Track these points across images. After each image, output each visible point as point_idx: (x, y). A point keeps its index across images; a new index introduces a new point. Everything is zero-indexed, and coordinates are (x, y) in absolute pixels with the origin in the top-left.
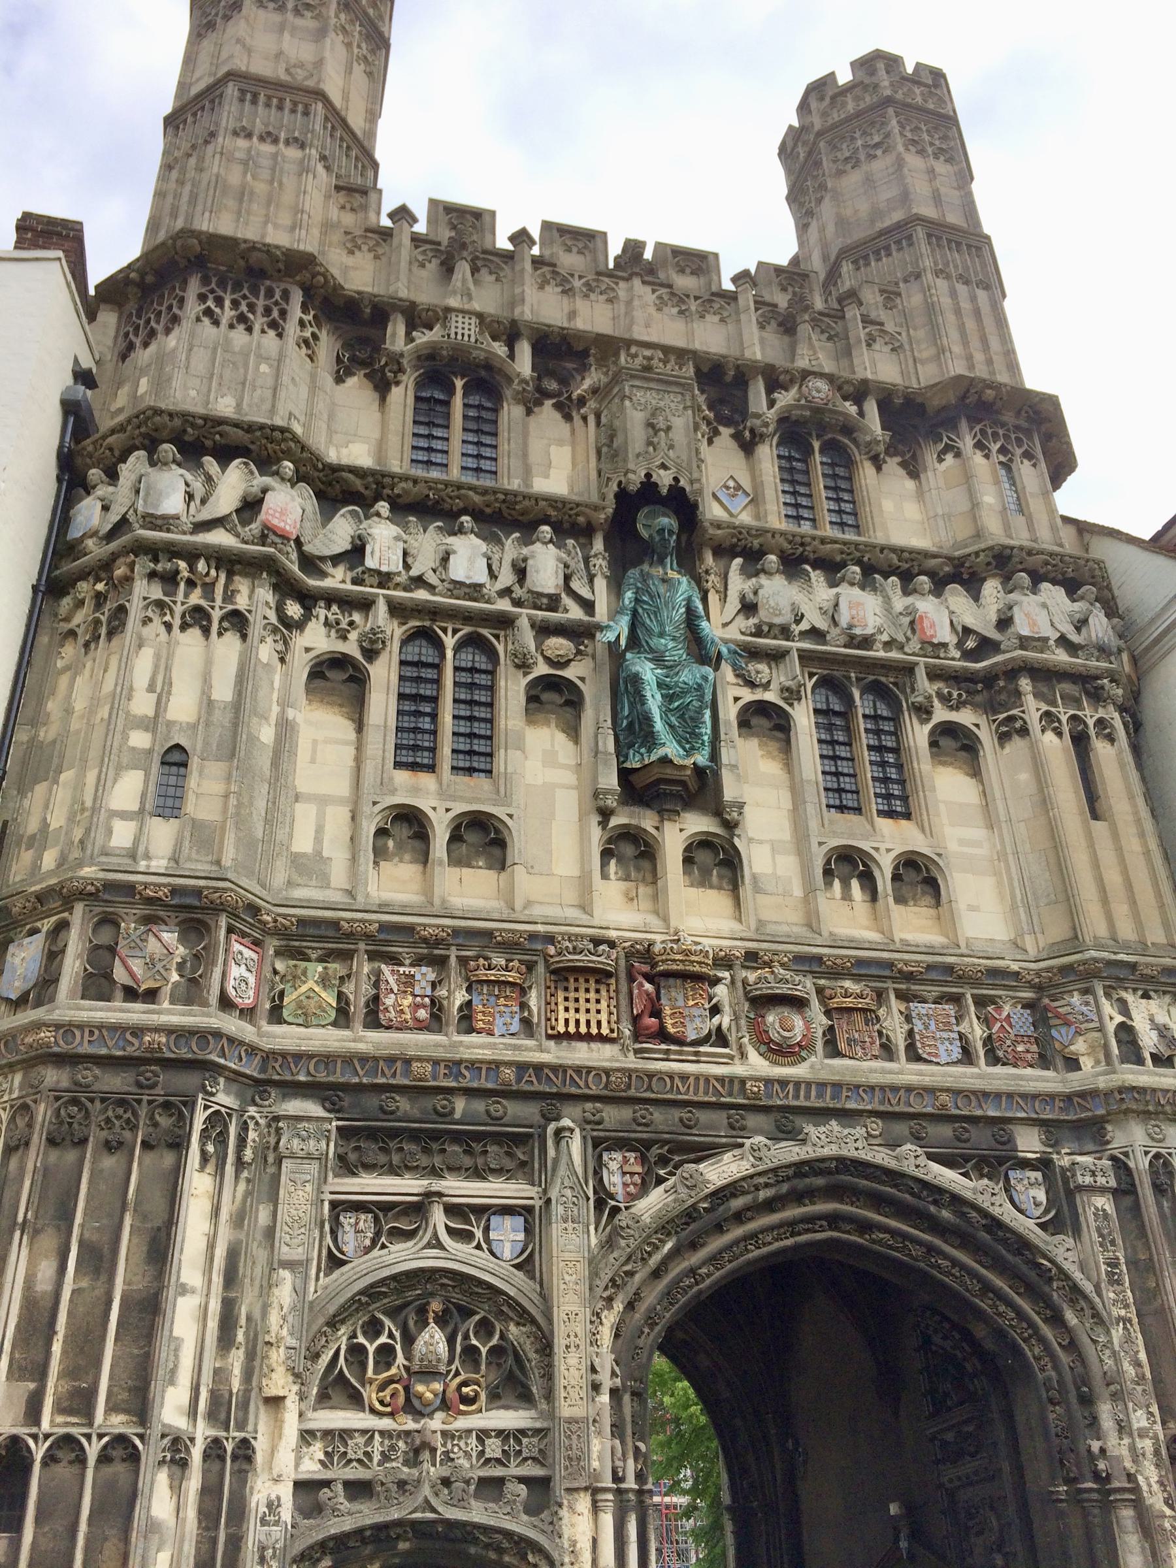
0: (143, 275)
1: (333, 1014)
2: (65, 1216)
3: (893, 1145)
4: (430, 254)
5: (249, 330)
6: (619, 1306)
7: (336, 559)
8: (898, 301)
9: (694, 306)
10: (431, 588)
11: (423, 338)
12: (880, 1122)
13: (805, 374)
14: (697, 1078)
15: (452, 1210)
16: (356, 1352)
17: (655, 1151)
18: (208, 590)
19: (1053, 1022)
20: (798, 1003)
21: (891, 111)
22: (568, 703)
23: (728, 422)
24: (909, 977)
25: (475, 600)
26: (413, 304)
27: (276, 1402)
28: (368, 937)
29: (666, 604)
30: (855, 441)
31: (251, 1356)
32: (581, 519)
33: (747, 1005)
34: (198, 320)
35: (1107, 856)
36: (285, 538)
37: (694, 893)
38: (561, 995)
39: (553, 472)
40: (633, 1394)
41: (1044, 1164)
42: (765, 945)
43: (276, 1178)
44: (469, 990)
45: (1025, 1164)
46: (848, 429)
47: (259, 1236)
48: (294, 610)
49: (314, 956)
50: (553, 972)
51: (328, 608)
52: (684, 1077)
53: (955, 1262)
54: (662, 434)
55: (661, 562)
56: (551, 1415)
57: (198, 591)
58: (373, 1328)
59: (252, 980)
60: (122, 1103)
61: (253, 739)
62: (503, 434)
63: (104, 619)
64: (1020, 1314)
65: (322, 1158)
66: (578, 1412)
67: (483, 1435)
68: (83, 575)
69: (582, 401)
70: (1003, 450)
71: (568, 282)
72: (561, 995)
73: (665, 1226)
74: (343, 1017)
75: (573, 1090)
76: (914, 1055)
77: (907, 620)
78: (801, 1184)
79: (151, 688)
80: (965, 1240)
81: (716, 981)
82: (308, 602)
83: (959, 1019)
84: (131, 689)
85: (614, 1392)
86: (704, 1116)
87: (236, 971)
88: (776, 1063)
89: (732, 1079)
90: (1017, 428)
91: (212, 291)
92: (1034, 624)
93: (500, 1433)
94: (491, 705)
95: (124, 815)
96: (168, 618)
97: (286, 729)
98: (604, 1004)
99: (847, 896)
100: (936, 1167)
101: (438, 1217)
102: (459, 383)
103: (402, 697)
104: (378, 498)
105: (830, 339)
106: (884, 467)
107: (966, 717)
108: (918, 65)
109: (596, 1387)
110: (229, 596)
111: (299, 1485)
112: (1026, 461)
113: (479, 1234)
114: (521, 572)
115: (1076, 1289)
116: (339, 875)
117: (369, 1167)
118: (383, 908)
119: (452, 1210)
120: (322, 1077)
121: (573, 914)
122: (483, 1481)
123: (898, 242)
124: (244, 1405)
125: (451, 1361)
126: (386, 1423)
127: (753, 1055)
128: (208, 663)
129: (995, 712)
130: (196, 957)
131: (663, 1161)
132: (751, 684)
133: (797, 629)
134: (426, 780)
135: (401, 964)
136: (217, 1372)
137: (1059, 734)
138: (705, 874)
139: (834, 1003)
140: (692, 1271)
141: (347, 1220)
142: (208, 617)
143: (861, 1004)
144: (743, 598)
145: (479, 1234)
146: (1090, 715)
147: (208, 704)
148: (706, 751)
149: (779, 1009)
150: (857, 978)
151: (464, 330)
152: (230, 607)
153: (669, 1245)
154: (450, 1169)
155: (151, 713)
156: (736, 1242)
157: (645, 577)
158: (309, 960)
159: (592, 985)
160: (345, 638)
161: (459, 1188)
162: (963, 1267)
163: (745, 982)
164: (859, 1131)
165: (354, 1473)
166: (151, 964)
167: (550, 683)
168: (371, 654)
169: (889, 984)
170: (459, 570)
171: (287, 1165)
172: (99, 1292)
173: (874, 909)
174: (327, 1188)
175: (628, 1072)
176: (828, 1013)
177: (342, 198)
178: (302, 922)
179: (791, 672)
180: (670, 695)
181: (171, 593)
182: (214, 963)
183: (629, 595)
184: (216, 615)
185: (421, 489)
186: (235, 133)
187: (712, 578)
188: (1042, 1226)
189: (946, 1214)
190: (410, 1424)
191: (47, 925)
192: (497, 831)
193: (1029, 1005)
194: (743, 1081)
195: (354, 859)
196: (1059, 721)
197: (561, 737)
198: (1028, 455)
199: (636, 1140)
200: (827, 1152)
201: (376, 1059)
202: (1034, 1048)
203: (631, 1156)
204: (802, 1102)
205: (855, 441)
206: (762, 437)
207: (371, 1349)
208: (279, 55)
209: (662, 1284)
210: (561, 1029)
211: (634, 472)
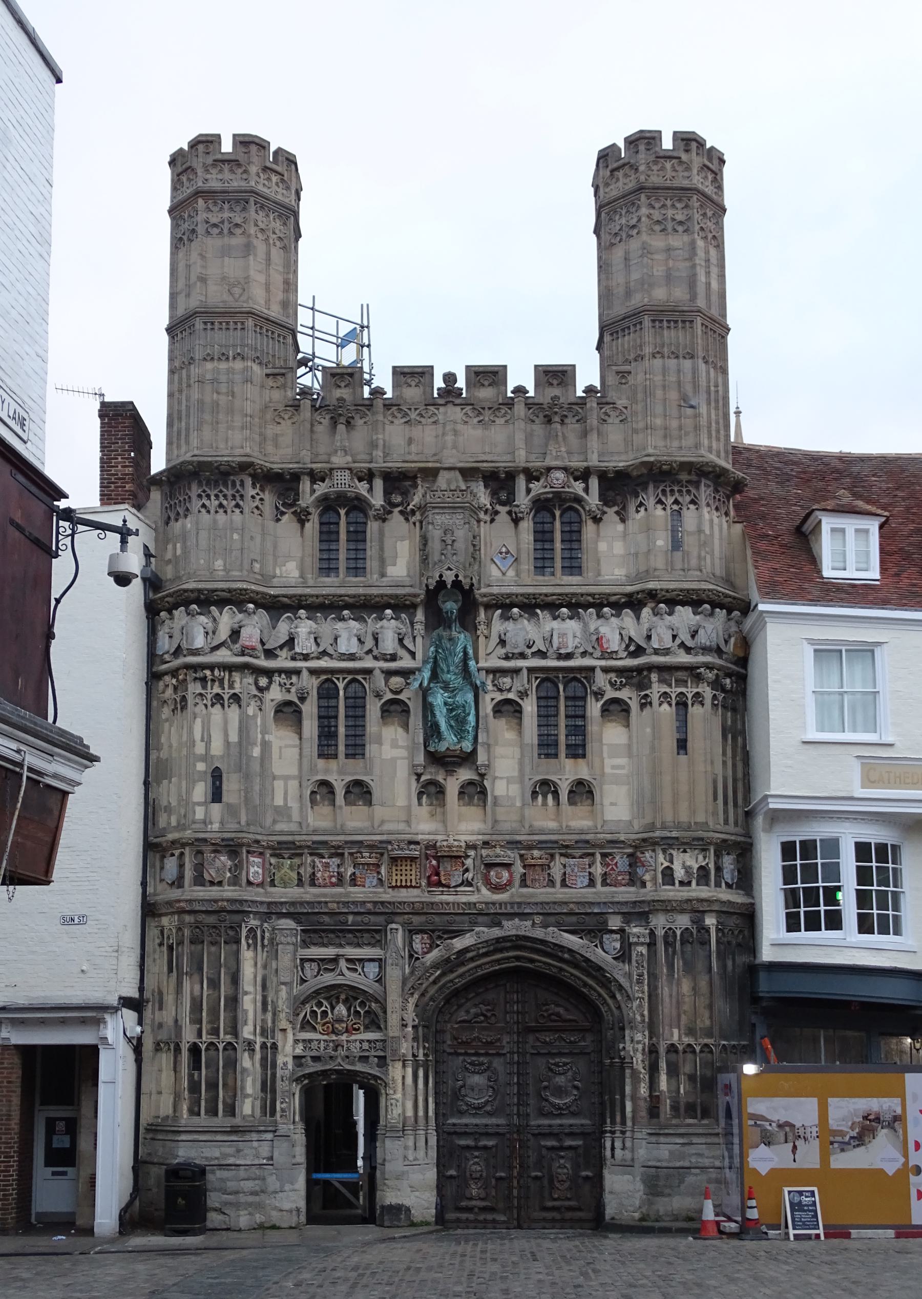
0: (168, 479)
1: (296, 882)
2: (201, 969)
3: (545, 926)
4: (324, 413)
5: (225, 512)
6: (416, 996)
7: (281, 647)
8: (629, 378)
9: (487, 413)
10: (330, 656)
11: (322, 488)
12: (541, 917)
13: (549, 469)
14: (453, 904)
15: (349, 961)
16: (314, 1013)
17: (437, 933)
18: (221, 681)
19: (639, 864)
20: (507, 866)
21: (643, 196)
22: (403, 711)
23: (503, 504)
24: (567, 847)
25: (353, 660)
26: (312, 470)
27: (284, 1030)
28: (308, 847)
29: (451, 654)
30: (584, 509)
31: (274, 1014)
32: (407, 602)
33: (483, 867)
34: (199, 512)
35: (683, 776)
36: (253, 649)
37: (464, 809)
38: (394, 868)
39: (398, 560)
40: (424, 1026)
41: (622, 931)
42: (494, 837)
43: (277, 950)
44: (354, 867)
45: (612, 932)
46: (578, 500)
47: (273, 972)
48: (263, 682)
49: (286, 856)
50: (392, 858)
51: (280, 676)
52: (448, 904)
53: (572, 975)
54: (449, 547)
55: (450, 628)
56: (385, 1035)
57: (217, 683)
58: (320, 1004)
59: (260, 871)
60: (215, 927)
61: (250, 757)
62: (368, 543)
63: (178, 700)
64: (600, 995)
65: (295, 945)
66: (396, 1034)
67: (361, 1041)
68: (166, 673)
69: (413, 512)
70: (676, 502)
71: (407, 414)
72: (394, 868)
73: (435, 966)
74: (300, 883)
75: (399, 911)
76: (564, 884)
77: (594, 637)
78: (500, 946)
79: (202, 740)
80: (576, 966)
81: (467, 856)
82: (270, 675)
83: (590, 866)
84: (194, 741)
85: (413, 1027)
86: (457, 918)
87: (252, 870)
88: (493, 893)
89: (469, 903)
90: (688, 482)
91: (204, 491)
92: (660, 640)
93: (368, 1041)
94: (364, 716)
95: (199, 804)
96: (205, 702)
97: (266, 746)
98: (413, 872)
99: (545, 804)
100: (566, 935)
101: (343, 964)
102: (342, 512)
103: (320, 717)
104: (301, 607)
105: (578, 421)
106: (605, 517)
107: (624, 694)
108: (675, 133)
109: (406, 1026)
110: (231, 686)
111: (295, 1057)
112: (692, 507)
113: (360, 970)
114: (376, 640)
115: (620, 985)
116: (296, 816)
117: (315, 944)
118: (315, 832)
119: (349, 961)
120: (292, 910)
121: (402, 827)
122: (361, 1057)
123: (635, 325)
124: (273, 1031)
125: (349, 1016)
126: (325, 1037)
127: (484, 891)
128: (226, 722)
129: (642, 690)
130: (236, 865)
131: (440, 937)
132: (501, 690)
133: (529, 652)
134: (333, 764)
135: (324, 858)
136: (262, 1020)
137: (670, 705)
138: (471, 798)
139: (527, 862)
140: (451, 981)
141: (307, 965)
142: (222, 698)
143: (540, 862)
144: (500, 636)
145: (360, 970)
146: (690, 691)
147: (227, 743)
148: (471, 737)
149: (497, 869)
150: (540, 849)
151: (342, 482)
152: (232, 691)
153: (438, 972)
154: (348, 944)
155: (204, 752)
156: (471, 969)
157: (440, 638)
158: (284, 858)
159: (409, 863)
160: (288, 691)
161: (352, 952)
162: (575, 976)
163: (482, 856)
164: (529, 923)
165: (314, 1053)
166: (218, 870)
167: (392, 702)
168: (302, 699)
169: (557, 851)
170: (343, 648)
171: (280, 947)
172: (217, 995)
173: (558, 809)
174: (298, 954)
175: (422, 903)
176: (524, 867)
177: (270, 382)
178: (279, 843)
179: (521, 682)
180: (451, 708)
181: (204, 687)
182: (242, 869)
183: (432, 649)
184: (226, 697)
185: (321, 600)
186: (205, 359)
187: (482, 628)
188: (614, 958)
189: (566, 956)
190: (334, 1038)
191: (177, 852)
192: (367, 787)
193: (630, 855)
194: (475, 904)
195: (301, 808)
196: (671, 698)
197: (400, 730)
198: (693, 502)
199: (430, 930)
200: (514, 932)
201: (312, 903)
202: (628, 877)
203: (425, 936)
204: (503, 911)
205: (584, 509)
206: (522, 519)
207: (319, 1012)
208: (224, 278)
209: (436, 987)
210: (394, 884)
211: (432, 577)
